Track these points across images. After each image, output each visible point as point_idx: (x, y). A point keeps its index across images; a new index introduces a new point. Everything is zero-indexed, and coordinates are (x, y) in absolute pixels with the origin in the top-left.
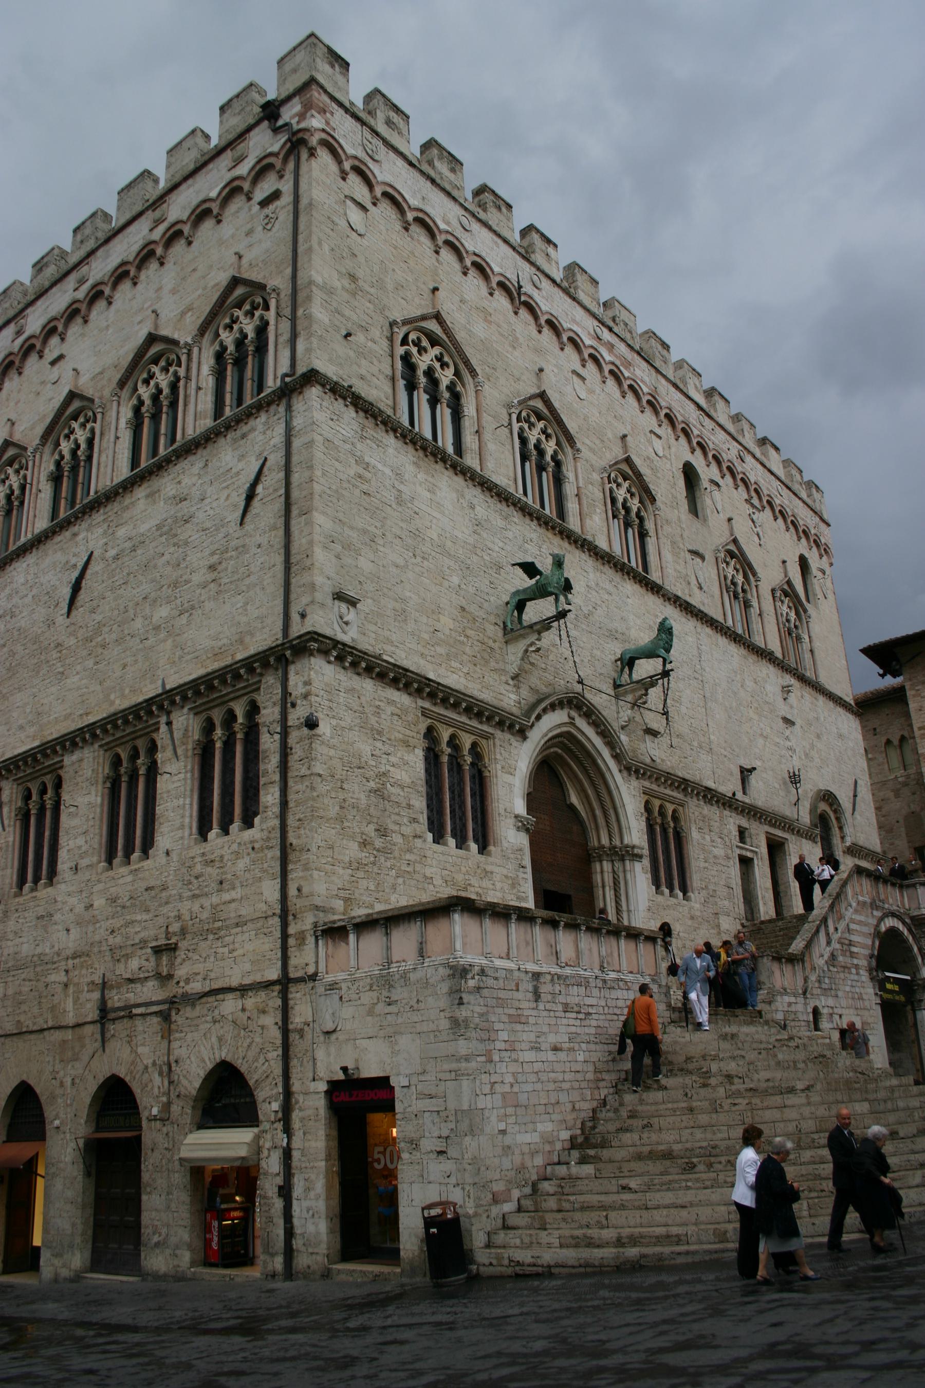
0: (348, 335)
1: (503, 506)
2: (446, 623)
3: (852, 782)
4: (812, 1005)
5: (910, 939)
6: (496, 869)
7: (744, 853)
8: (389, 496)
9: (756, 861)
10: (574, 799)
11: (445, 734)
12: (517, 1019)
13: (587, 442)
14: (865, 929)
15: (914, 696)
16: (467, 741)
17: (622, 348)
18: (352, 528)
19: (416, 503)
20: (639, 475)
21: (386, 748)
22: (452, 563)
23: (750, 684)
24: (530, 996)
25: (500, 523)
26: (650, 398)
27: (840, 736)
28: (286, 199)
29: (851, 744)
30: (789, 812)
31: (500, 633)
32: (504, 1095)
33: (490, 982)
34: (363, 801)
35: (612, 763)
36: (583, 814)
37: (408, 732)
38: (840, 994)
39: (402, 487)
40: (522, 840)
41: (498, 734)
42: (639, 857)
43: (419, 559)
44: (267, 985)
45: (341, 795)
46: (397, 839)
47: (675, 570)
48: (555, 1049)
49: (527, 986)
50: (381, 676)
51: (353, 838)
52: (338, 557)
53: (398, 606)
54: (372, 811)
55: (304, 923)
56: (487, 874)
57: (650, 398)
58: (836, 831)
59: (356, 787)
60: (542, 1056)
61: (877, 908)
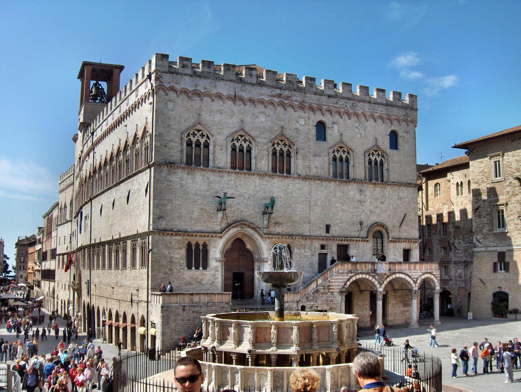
0: (166, 146)
1: (221, 174)
2: (196, 214)
3: (403, 216)
4: (301, 305)
5: (374, 280)
6: (207, 273)
7: (322, 252)
8: (178, 187)
9: (328, 254)
10: (248, 246)
11: (194, 243)
12: (178, 315)
13: (264, 136)
14: (342, 281)
15: (472, 166)
16: (201, 243)
17: (286, 93)
18: (164, 200)
19: (187, 185)
20: (287, 138)
21: (173, 251)
22: (199, 198)
23: (338, 194)
24: (182, 310)
25: (219, 179)
26: (300, 105)
27: (400, 198)
28: (152, 105)
29: (407, 200)
30: (353, 234)
31: (216, 211)
32: (172, 329)
33: (170, 308)
34: (165, 264)
35: (258, 237)
36: (251, 250)
37: (180, 245)
38: (318, 301)
39: (183, 182)
40: (218, 264)
41: (212, 238)
42: (267, 262)
43: (187, 200)
44: (145, 302)
45: (159, 264)
46: (176, 271)
47: (303, 166)
48: (188, 320)
49: (181, 308)
50: (172, 235)
51: (162, 273)
52: (160, 209)
53: (179, 215)
54: (168, 266)
55: (150, 291)
56: (204, 274)
57: (300, 105)
58: (385, 235)
59: (163, 262)
60: (185, 322)
61: (351, 273)
